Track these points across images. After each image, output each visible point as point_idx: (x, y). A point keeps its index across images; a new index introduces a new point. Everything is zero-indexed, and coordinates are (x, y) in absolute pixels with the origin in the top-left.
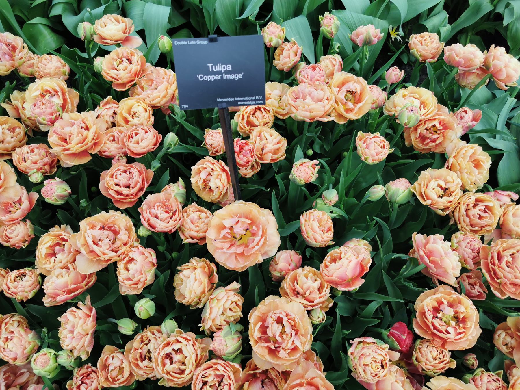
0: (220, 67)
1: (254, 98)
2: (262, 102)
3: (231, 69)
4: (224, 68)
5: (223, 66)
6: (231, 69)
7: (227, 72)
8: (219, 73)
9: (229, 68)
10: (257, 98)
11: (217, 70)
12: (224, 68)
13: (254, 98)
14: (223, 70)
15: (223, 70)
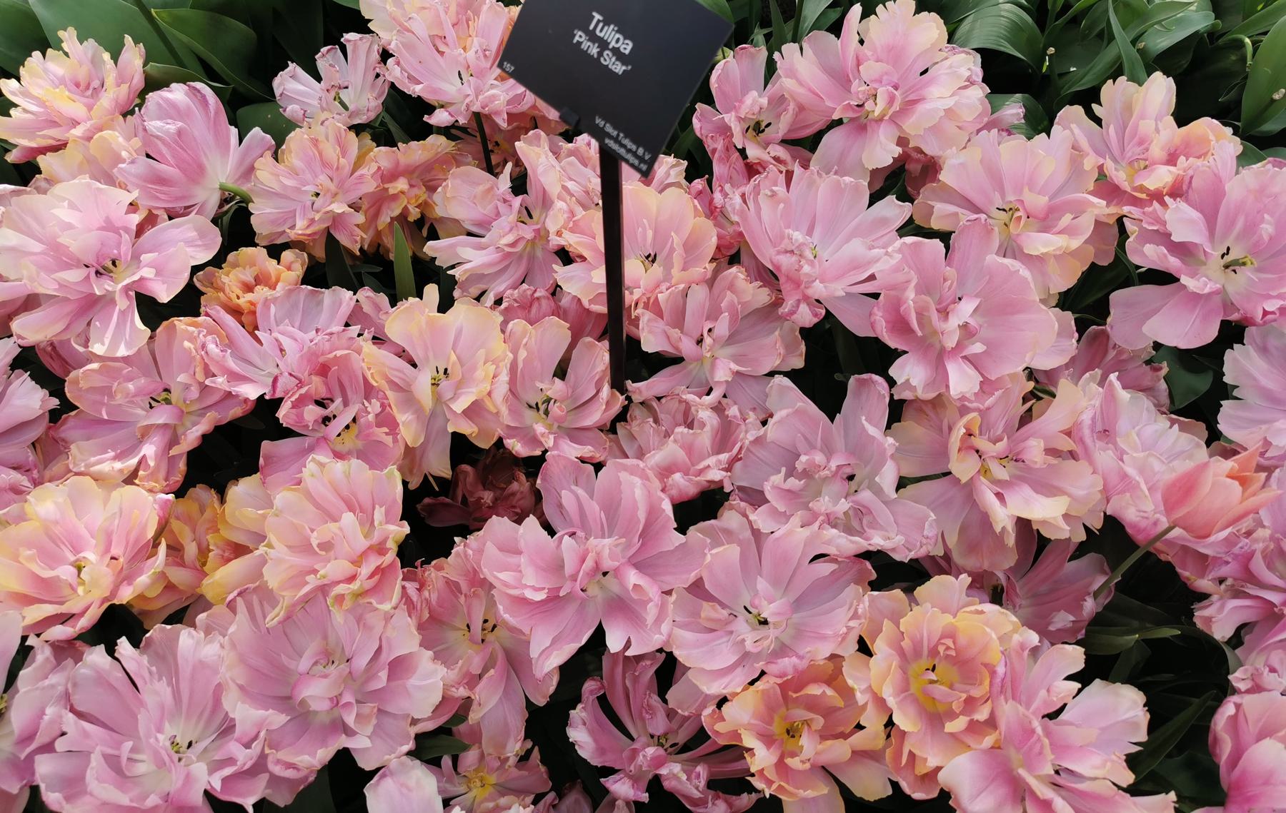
0: (610, 34)
1: (634, 148)
2: (644, 167)
3: (627, 52)
4: (618, 41)
5: (618, 36)
6: (627, 52)
7: (616, 52)
8: (603, 44)
9: (627, 47)
10: (641, 151)
11: (601, 35)
12: (618, 41)
13: (634, 148)
14: (613, 44)
15: (613, 44)
